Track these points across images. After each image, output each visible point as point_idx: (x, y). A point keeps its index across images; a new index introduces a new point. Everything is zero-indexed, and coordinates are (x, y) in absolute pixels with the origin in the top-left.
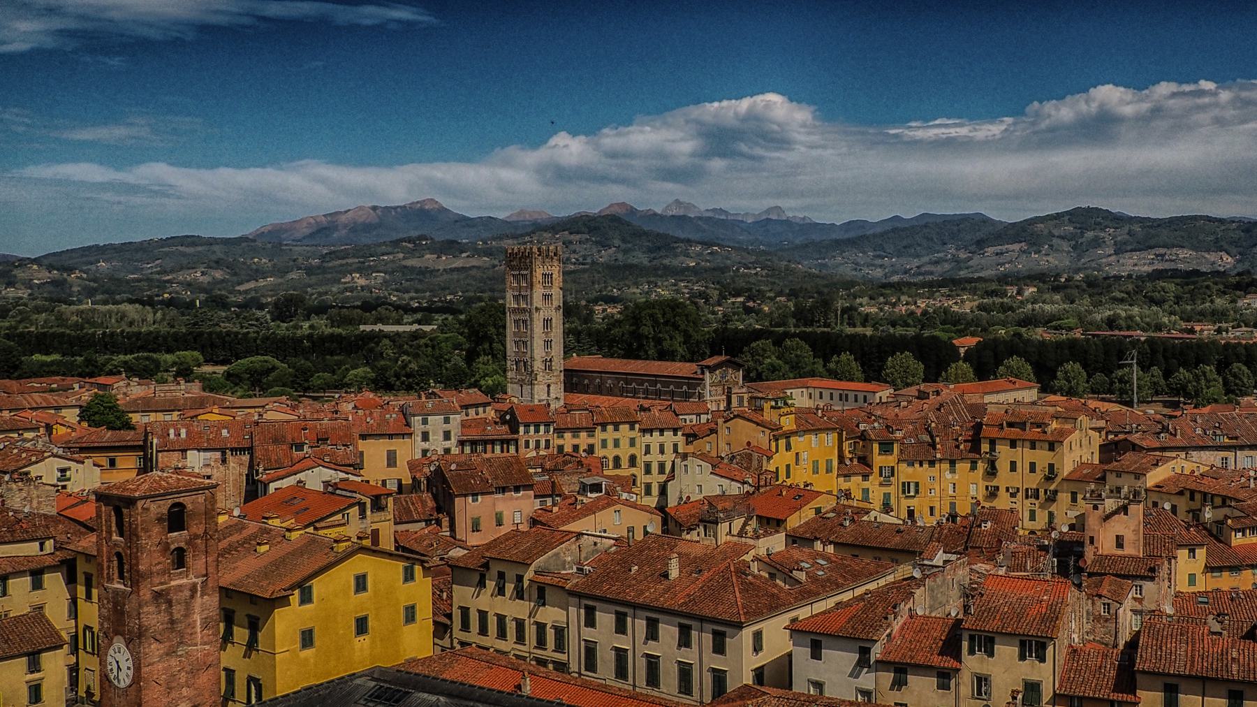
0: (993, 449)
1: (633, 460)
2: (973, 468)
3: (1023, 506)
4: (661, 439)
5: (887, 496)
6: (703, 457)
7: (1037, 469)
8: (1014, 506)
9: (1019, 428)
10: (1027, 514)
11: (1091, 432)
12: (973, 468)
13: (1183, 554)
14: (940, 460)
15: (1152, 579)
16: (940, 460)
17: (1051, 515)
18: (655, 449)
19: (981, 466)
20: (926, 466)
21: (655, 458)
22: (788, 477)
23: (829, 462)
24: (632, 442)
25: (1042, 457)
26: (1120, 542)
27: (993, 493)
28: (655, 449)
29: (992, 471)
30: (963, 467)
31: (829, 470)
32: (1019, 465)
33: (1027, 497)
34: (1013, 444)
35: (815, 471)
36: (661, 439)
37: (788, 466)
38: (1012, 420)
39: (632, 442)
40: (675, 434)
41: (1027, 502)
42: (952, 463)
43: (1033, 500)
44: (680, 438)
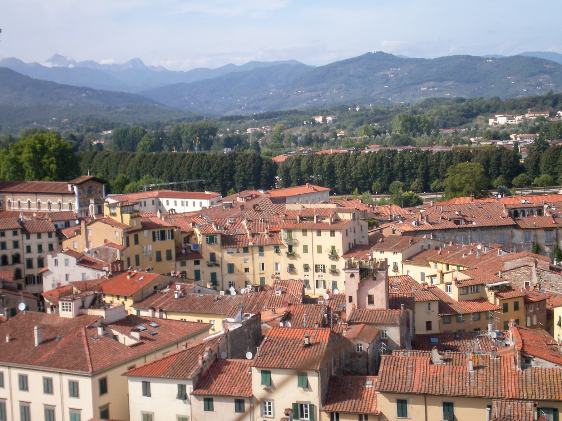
0: (290, 237)
1: (16, 259)
4: (39, 241)
5: (214, 275)
6: (70, 252)
8: (307, 278)
9: (308, 222)
11: (362, 222)
12: (277, 252)
14: (252, 247)
17: (334, 284)
18: (34, 249)
19: (284, 250)
20: (241, 250)
21: (34, 255)
22: (138, 263)
23: (169, 252)
24: (16, 245)
27: (291, 269)
28: (34, 249)
29: (291, 254)
31: (169, 258)
32: (310, 249)
33: (317, 271)
34: (305, 231)
35: (159, 259)
36: (39, 241)
37: (137, 257)
39: (16, 245)
40: (50, 235)
41: (316, 275)
42: (261, 249)
44: (54, 240)
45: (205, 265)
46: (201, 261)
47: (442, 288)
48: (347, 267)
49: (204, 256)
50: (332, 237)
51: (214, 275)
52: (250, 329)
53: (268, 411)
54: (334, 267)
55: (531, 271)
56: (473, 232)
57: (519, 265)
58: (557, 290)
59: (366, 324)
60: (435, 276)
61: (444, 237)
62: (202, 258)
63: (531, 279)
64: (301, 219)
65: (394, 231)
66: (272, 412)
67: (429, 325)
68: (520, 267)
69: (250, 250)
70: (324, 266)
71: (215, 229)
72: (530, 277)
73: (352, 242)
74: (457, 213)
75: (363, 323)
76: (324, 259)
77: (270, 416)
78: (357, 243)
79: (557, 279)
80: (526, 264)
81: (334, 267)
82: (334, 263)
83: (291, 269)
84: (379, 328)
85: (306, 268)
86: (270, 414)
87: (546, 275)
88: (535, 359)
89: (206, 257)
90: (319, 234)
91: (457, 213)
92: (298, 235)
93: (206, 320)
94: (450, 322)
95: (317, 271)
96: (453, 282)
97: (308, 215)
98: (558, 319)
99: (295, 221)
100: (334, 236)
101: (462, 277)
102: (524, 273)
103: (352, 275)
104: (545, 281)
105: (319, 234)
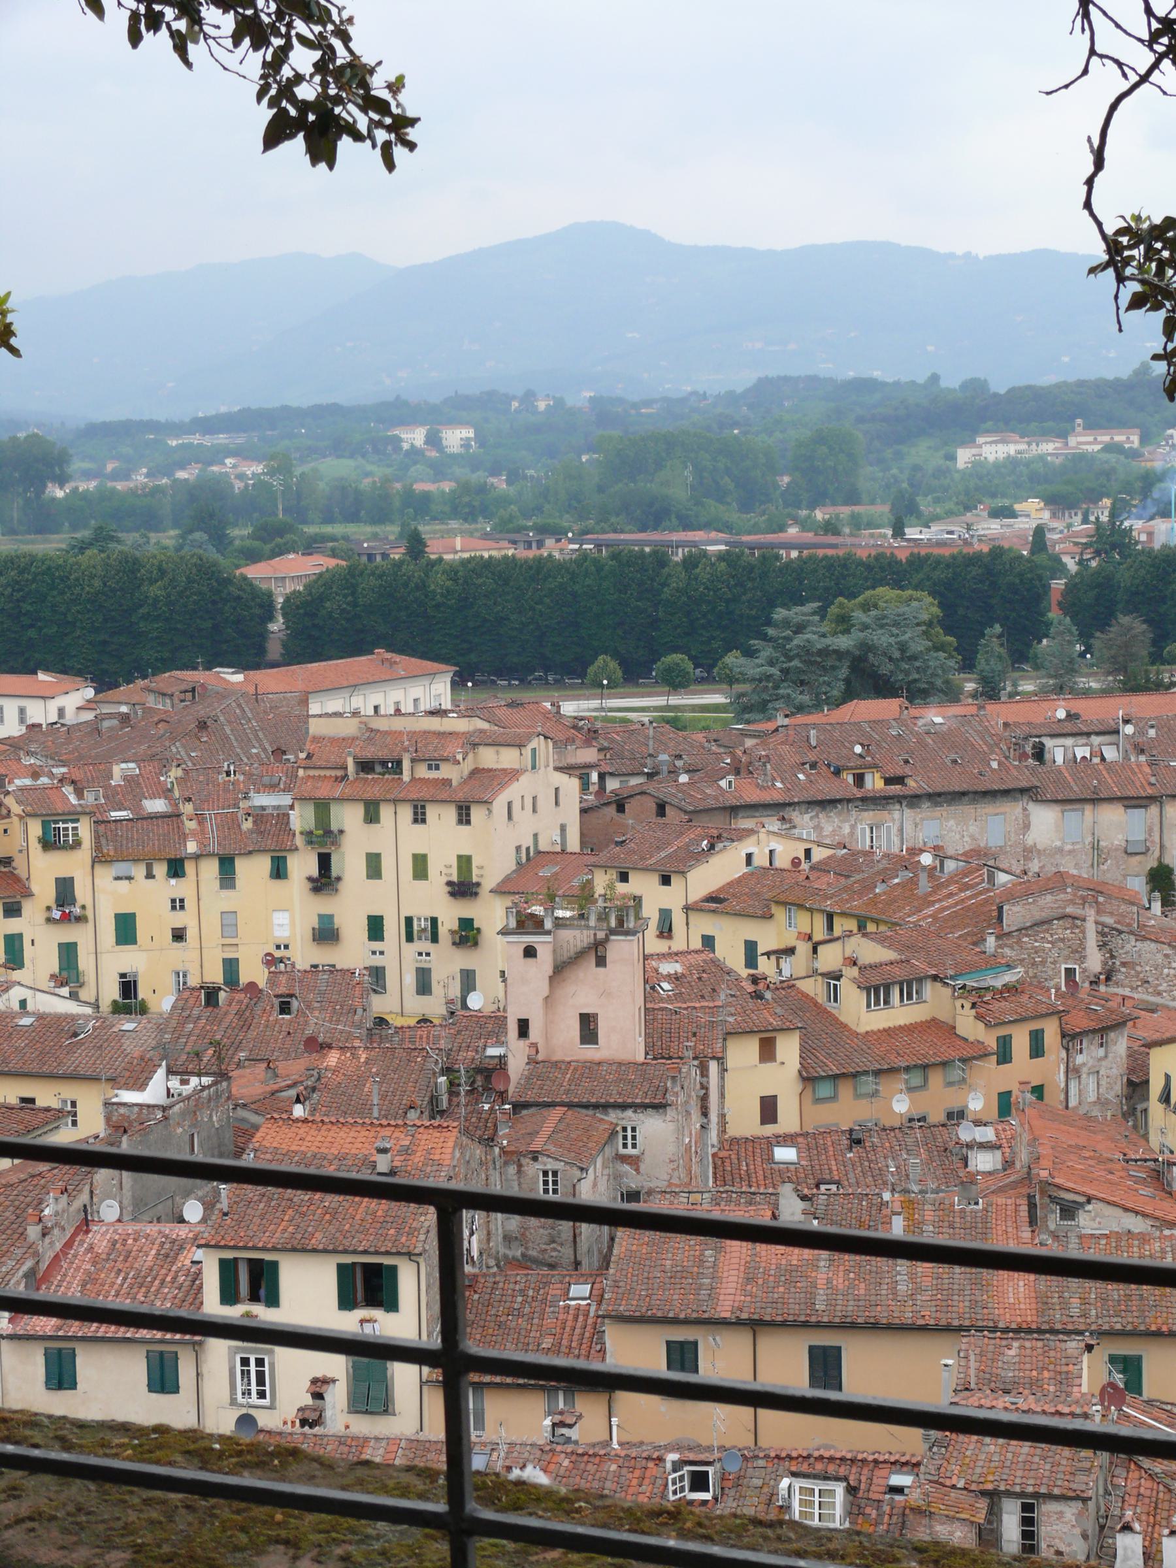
2: (279, 871)
3: (399, 958)
5: (68, 952)
7: (433, 869)
8: (377, 961)
10: (410, 979)
12: (279, 871)
13: (742, 1053)
14: (197, 857)
15: (660, 1107)
16: (197, 857)
19: (303, 865)
20: (160, 869)
25: (443, 839)
26: (588, 1027)
27: (326, 933)
29: (325, 880)
30: (253, 870)
32: (387, 865)
38: (369, 753)
41: (410, 950)
43: (425, 945)
45: (41, 917)
46: (27, 907)
47: (814, 988)
48: (513, 924)
49: (35, 888)
50: (464, 829)
51: (68, 952)
52: (193, 1125)
53: (254, 1388)
54: (466, 924)
55: (1083, 932)
56: (908, 812)
57: (1044, 915)
58: (1159, 994)
59: (570, 1105)
60: (790, 951)
61: (818, 828)
62: (28, 894)
63: (1083, 959)
64: (365, 766)
65: (661, 810)
66: (267, 1388)
67: (769, 1109)
68: (1048, 922)
69: (189, 867)
70: (434, 921)
71: (73, 799)
72: (1078, 952)
73: (528, 842)
74: (858, 749)
75: (562, 1104)
76: (431, 900)
77: (262, 1402)
78: (543, 847)
79: (1159, 958)
80: (1069, 910)
81: (466, 924)
82: (465, 909)
83: (326, 933)
84: (613, 1116)
85: (375, 927)
86: (262, 1395)
87: (1128, 947)
88: (1089, 1207)
89: (44, 891)
90: (419, 818)
91: (858, 749)
92: (348, 817)
93: (47, 1096)
94: (834, 1098)
95: (410, 938)
96: (852, 972)
97: (382, 754)
98: (1162, 1082)
99: (340, 773)
100: (468, 822)
101: (872, 952)
102: (1062, 940)
103: (530, 952)
104: (1124, 964)
105: (419, 818)
